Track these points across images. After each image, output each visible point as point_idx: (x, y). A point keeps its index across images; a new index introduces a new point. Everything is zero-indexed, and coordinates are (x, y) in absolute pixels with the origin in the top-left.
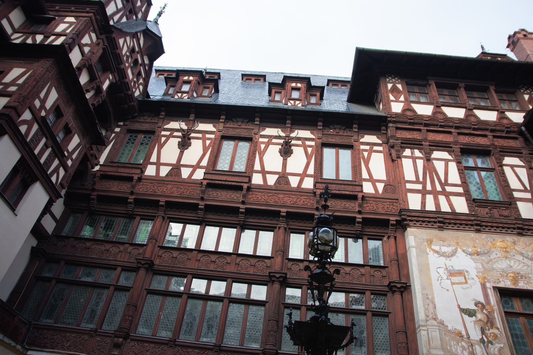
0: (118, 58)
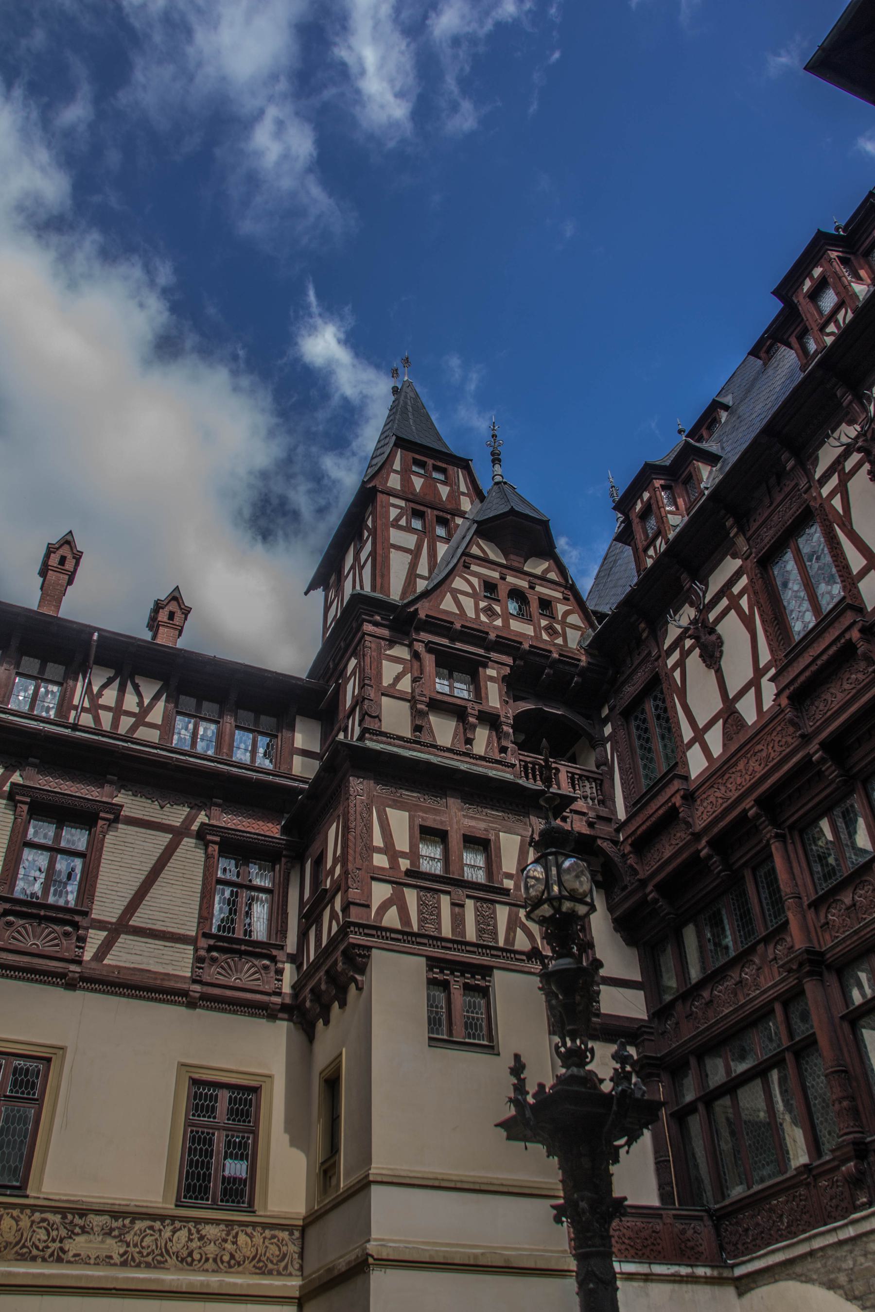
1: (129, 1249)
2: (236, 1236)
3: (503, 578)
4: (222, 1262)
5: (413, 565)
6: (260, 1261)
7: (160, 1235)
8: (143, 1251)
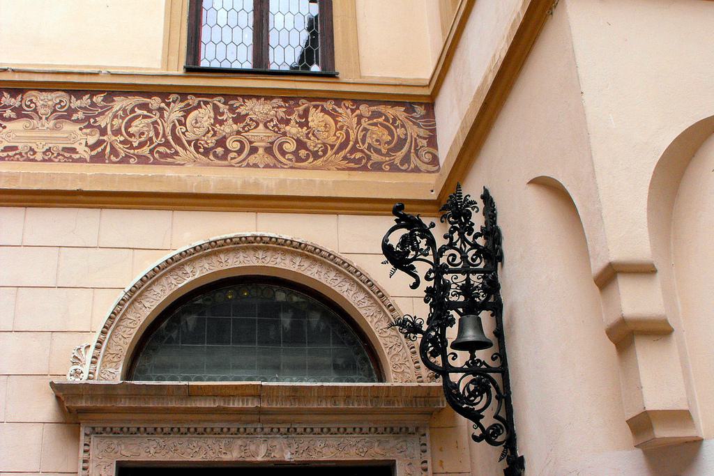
1: (105, 138)
2: (306, 113)
4: (283, 153)
7: (162, 116)
8: (132, 139)
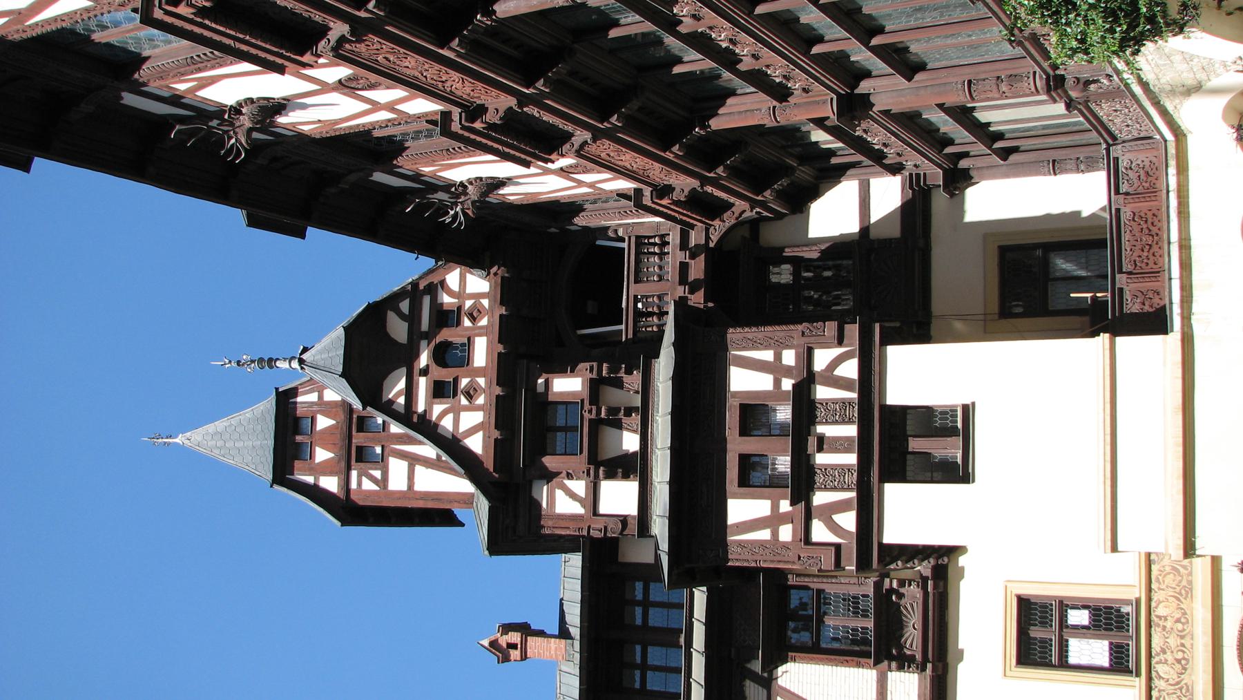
0: (503, 414)
2: (1159, 617)
3: (424, 372)
5: (426, 462)
6: (1180, 594)
